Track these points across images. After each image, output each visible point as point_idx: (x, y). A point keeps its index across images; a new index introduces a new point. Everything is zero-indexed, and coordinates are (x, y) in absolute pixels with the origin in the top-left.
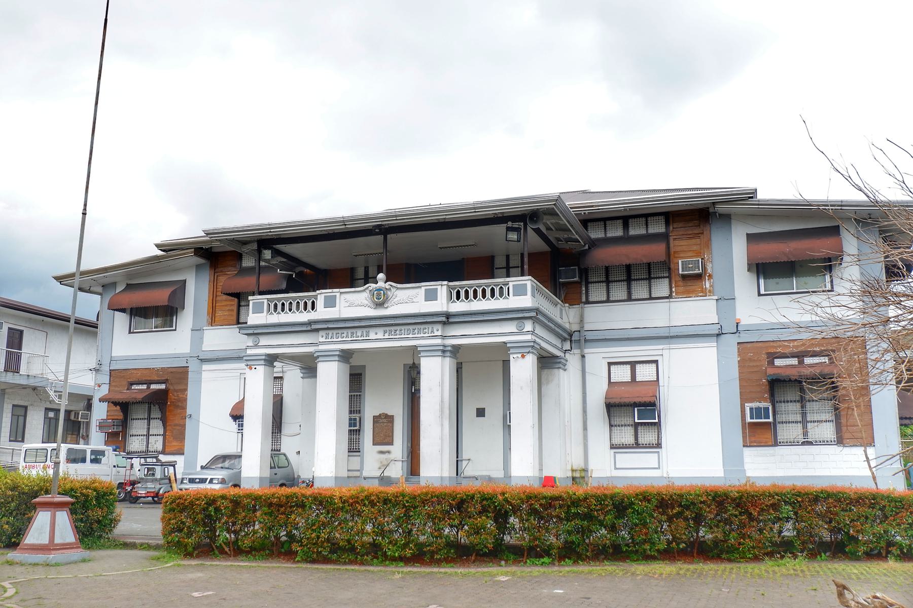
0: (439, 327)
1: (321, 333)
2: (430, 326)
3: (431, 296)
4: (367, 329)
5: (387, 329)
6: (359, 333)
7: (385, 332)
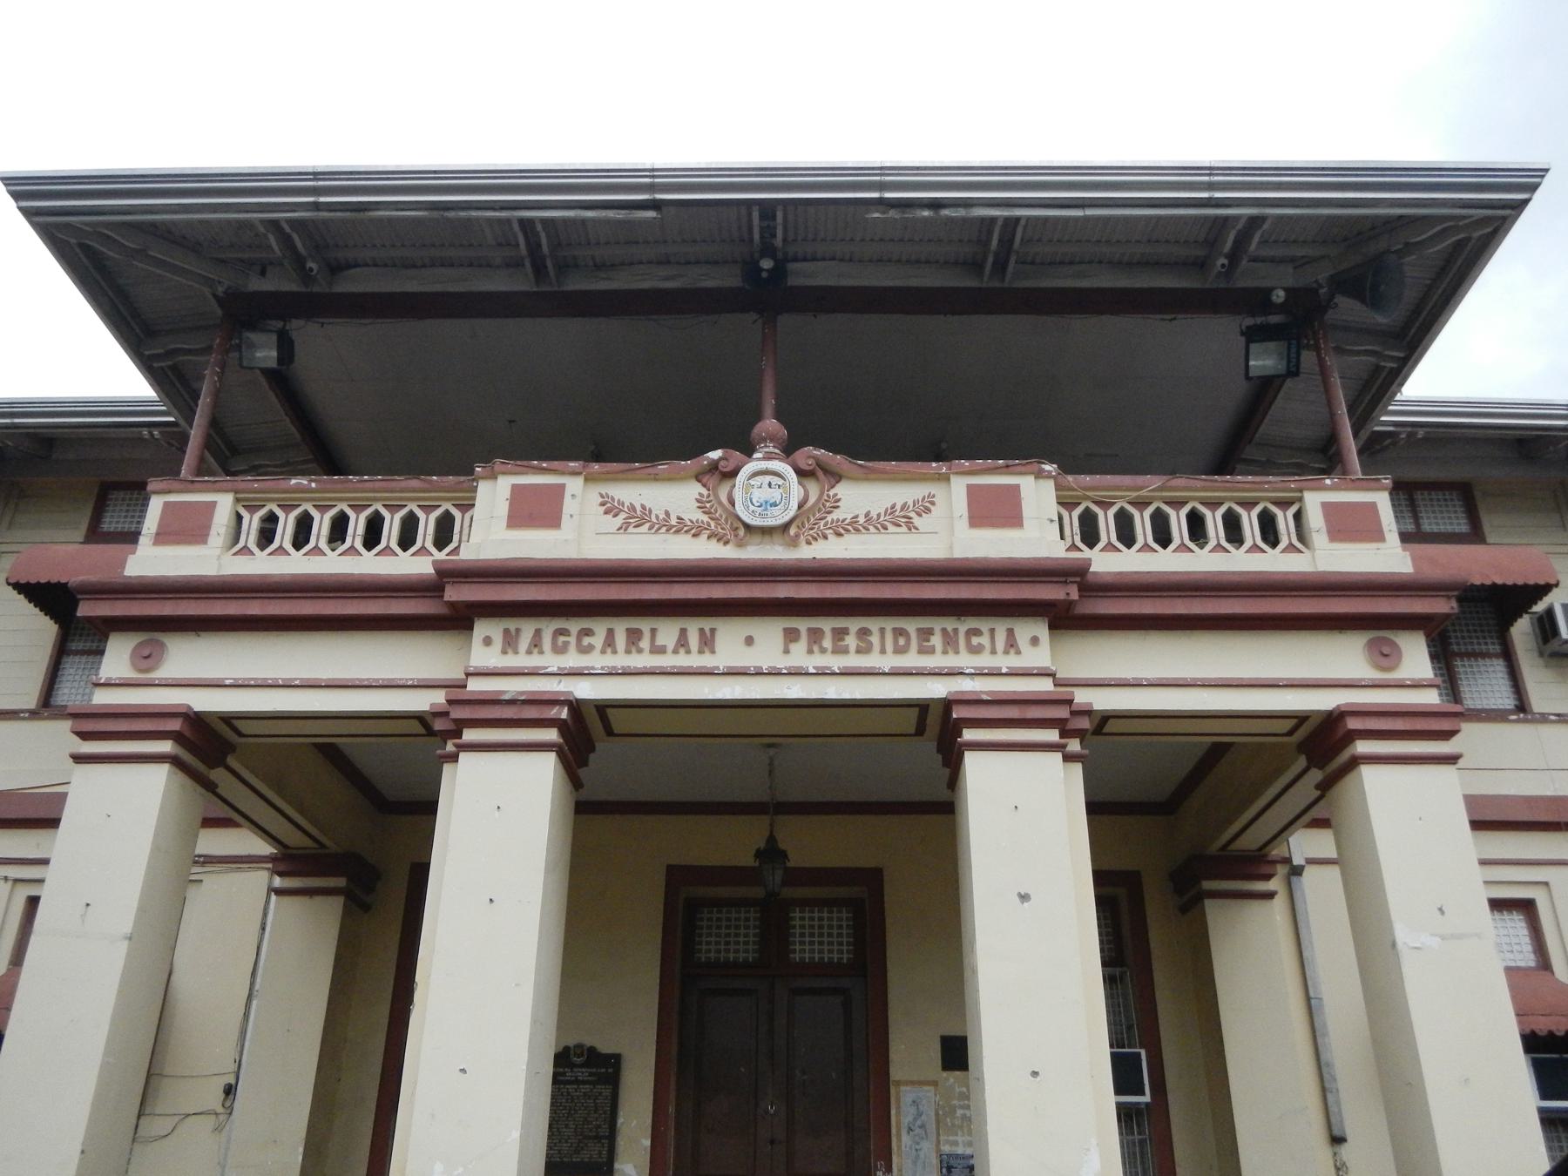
0: (1041, 629)
1: (482, 628)
2: (1001, 627)
3: (996, 510)
4: (707, 623)
5: (803, 624)
6: (668, 631)
7: (791, 636)
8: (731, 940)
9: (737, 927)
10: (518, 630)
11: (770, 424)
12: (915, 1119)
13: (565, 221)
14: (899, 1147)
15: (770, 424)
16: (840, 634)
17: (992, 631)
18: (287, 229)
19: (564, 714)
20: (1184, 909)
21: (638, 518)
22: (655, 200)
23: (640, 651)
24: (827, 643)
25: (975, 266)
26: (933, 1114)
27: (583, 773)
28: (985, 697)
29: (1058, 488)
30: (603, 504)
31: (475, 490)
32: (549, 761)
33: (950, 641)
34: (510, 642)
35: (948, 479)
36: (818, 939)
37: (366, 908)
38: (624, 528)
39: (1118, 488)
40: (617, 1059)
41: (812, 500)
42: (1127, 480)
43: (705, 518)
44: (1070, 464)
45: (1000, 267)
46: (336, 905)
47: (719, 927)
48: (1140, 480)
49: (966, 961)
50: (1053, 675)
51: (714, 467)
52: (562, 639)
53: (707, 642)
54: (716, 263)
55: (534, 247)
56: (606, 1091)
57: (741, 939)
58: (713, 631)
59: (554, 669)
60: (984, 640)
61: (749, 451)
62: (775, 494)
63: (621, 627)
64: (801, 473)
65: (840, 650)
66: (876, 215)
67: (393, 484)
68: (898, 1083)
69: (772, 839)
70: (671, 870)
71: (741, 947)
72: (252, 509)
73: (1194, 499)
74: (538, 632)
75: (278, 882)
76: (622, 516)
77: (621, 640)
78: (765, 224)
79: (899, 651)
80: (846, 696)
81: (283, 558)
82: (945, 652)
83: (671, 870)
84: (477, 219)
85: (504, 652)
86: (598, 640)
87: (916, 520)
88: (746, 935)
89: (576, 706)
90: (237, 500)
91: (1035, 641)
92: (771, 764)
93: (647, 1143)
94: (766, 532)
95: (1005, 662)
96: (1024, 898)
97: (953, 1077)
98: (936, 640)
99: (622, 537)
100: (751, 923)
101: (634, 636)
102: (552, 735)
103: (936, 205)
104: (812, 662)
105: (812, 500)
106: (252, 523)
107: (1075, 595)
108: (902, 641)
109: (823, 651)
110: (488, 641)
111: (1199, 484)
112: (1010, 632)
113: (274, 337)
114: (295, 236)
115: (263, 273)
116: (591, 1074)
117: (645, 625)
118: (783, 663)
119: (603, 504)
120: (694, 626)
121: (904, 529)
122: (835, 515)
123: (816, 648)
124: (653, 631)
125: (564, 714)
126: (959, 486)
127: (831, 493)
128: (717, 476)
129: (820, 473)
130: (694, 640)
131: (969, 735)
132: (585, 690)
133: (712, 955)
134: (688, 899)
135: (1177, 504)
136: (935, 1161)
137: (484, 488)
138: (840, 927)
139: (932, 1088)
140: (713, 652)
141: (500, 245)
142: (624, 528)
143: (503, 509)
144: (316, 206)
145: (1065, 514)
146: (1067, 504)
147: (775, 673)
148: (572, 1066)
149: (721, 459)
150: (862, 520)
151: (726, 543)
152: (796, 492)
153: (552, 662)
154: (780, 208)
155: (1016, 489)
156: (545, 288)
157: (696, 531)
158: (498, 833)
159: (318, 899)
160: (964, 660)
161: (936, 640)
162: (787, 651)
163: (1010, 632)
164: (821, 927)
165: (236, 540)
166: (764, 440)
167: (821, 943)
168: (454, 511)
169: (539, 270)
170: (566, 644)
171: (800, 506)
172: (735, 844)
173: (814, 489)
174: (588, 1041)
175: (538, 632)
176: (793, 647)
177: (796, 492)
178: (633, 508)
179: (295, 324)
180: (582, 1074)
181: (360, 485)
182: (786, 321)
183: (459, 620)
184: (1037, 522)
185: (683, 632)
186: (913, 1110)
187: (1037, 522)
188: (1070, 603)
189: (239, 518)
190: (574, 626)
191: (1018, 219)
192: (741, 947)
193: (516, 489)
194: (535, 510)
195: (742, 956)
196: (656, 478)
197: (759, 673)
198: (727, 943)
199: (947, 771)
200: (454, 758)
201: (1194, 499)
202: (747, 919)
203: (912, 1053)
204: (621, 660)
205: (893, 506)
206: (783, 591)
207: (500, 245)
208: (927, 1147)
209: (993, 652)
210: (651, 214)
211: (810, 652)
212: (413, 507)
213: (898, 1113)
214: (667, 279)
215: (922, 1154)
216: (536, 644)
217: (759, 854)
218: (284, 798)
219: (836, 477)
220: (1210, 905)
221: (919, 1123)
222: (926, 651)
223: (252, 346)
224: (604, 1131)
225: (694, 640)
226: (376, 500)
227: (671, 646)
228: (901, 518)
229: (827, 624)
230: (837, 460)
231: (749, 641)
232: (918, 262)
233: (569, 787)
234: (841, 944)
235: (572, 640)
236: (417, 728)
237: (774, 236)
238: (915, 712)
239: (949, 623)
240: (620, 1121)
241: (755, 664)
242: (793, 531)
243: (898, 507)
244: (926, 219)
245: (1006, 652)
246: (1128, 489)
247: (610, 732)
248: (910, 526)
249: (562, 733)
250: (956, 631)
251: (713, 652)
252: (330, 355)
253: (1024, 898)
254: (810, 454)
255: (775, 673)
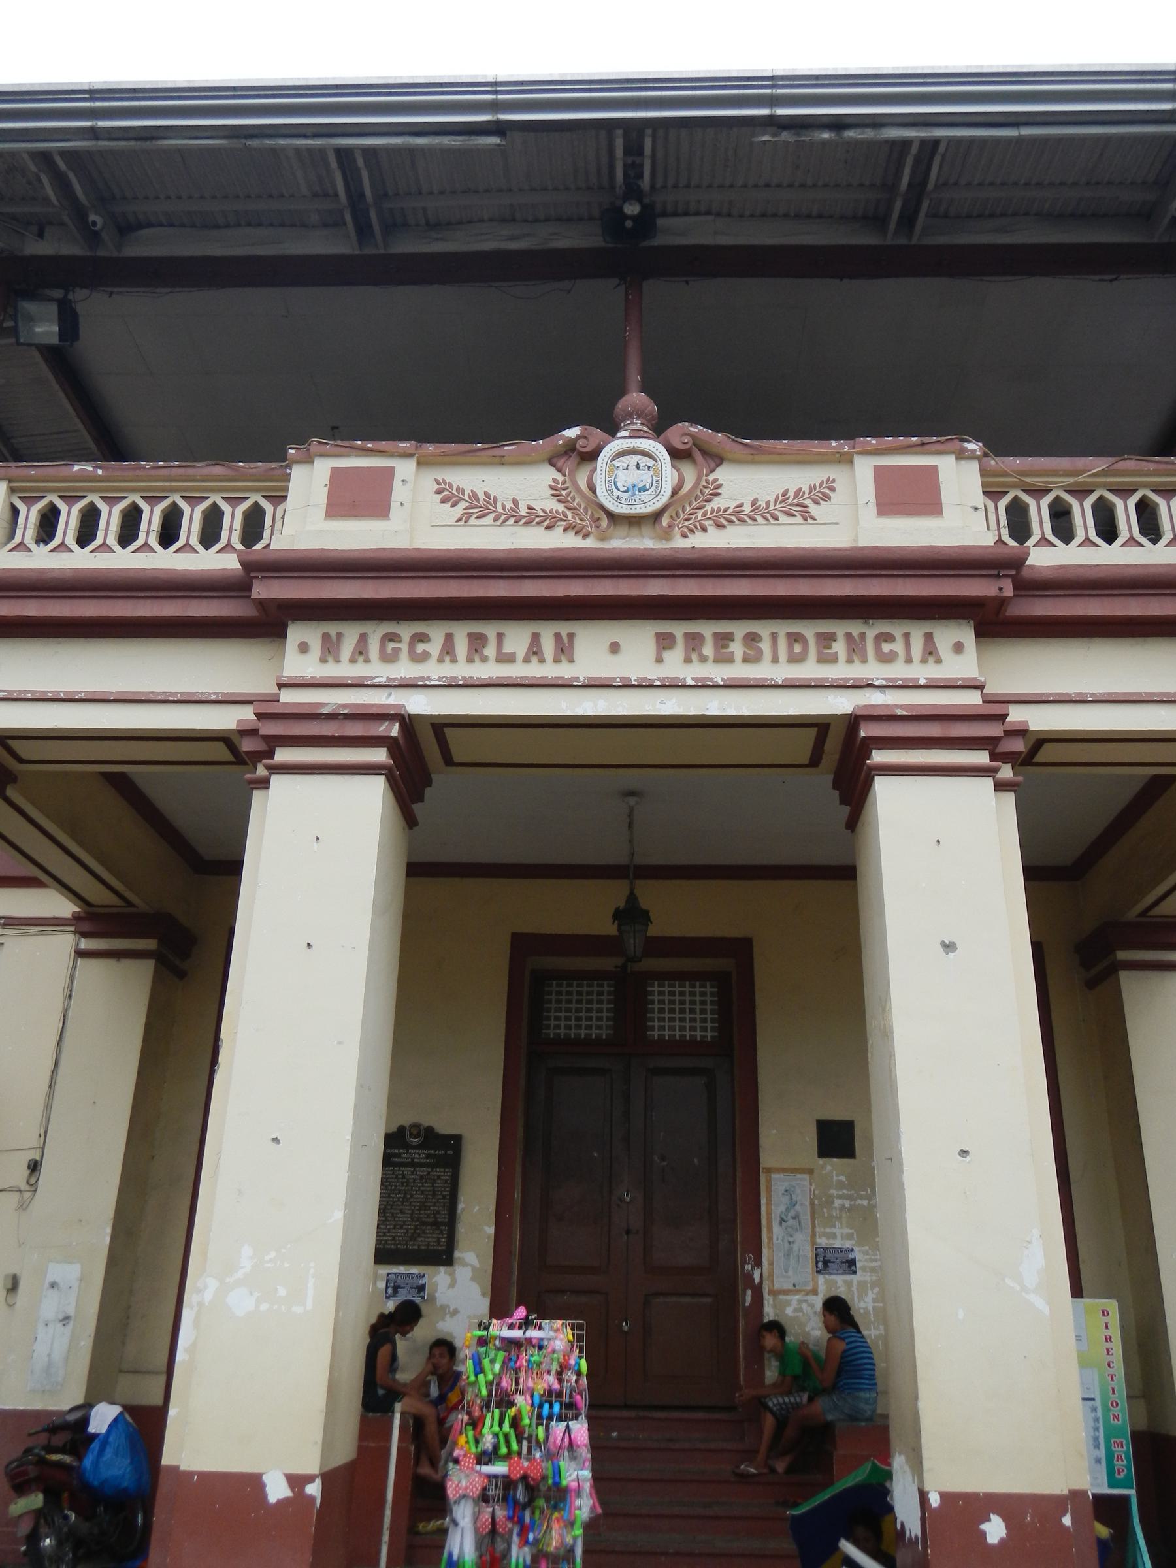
0: (965, 634)
1: (296, 633)
2: (917, 631)
3: (910, 495)
4: (564, 628)
5: (679, 629)
6: (517, 636)
7: (665, 642)
8: (583, 1015)
9: (589, 1002)
10: (339, 635)
11: (636, 398)
12: (788, 1210)
13: (388, 150)
14: (770, 1239)
15: (636, 398)
16: (723, 639)
17: (907, 636)
18: (62, 165)
19: (395, 731)
20: (1091, 984)
21: (482, 508)
22: (498, 122)
23: (484, 660)
24: (708, 650)
25: (877, 220)
26: (808, 1203)
27: (417, 808)
28: (899, 712)
29: (984, 473)
30: (439, 492)
31: (287, 478)
32: (377, 786)
33: (856, 649)
34: (330, 649)
35: (851, 462)
36: (680, 1014)
37: (181, 975)
38: (464, 519)
39: (1055, 473)
40: (458, 1139)
41: (688, 486)
42: (1064, 463)
43: (561, 508)
44: (1000, 443)
45: (908, 220)
46: (146, 968)
47: (569, 1002)
48: (1080, 462)
49: (872, 1025)
50: (980, 687)
51: (570, 448)
52: (391, 645)
53: (564, 650)
54: (569, 220)
55: (356, 198)
56: (445, 1174)
57: (594, 1015)
58: (571, 636)
59: (382, 680)
60: (898, 647)
61: (612, 430)
62: (645, 478)
63: (461, 631)
64: (677, 455)
65: (725, 659)
66: (765, 138)
67: (190, 471)
68: (769, 1171)
69: (632, 898)
70: (517, 938)
71: (594, 1023)
72: (29, 500)
73: (1145, 485)
74: (363, 638)
75: (84, 944)
76: (462, 505)
77: (461, 647)
78: (629, 160)
79: (794, 659)
80: (732, 711)
81: (65, 555)
82: (850, 661)
83: (517, 938)
84: (283, 149)
85: (323, 660)
86: (434, 647)
87: (813, 509)
88: (599, 1011)
89: (408, 722)
90: (12, 490)
91: (958, 648)
92: (630, 815)
93: (491, 1230)
94: (634, 521)
95: (923, 672)
96: (949, 947)
97: (833, 1167)
98: (839, 647)
99: (462, 530)
100: (605, 997)
101: (477, 643)
102: (380, 756)
103: (838, 124)
104: (691, 673)
105: (688, 486)
106: (30, 516)
107: (1009, 592)
108: (797, 648)
109: (703, 659)
110: (304, 648)
111: (1152, 467)
112: (929, 637)
113: (54, 308)
114: (71, 175)
115: (41, 235)
116: (428, 1156)
117: (489, 629)
118: (655, 673)
119: (439, 492)
120: (548, 632)
121: (799, 519)
122: (717, 503)
123: (694, 657)
124: (500, 637)
125: (395, 731)
126: (864, 469)
127: (711, 478)
128: (574, 459)
129: (697, 455)
130: (548, 646)
131: (879, 757)
132: (418, 704)
133: (562, 1031)
134: (536, 971)
135: (1124, 492)
136: (810, 1254)
137: (298, 474)
138: (703, 1003)
139: (807, 1176)
140: (572, 661)
141: (315, 195)
142: (464, 519)
143: (321, 495)
144: (94, 133)
145: (990, 505)
146: (992, 494)
147: (645, 685)
148: (408, 1147)
149: (578, 437)
150: (747, 509)
151: (586, 536)
152: (669, 476)
153: (380, 671)
154: (649, 131)
155: (935, 469)
156: (368, 251)
157: (550, 522)
158: (317, 874)
159: (127, 963)
160: (873, 670)
161: (839, 647)
162: (659, 660)
163: (929, 637)
164: (682, 1002)
165: (12, 536)
166: (630, 415)
167: (682, 1020)
168: (265, 504)
169: (363, 231)
170: (397, 651)
171: (674, 493)
172: (589, 911)
173: (690, 474)
174: (426, 1121)
175: (363, 638)
176: (667, 655)
177: (669, 476)
178: (474, 495)
179: (79, 294)
180: (419, 1155)
181: (153, 472)
182: (653, 288)
183: (269, 626)
184: (961, 508)
185: (536, 637)
186: (785, 1200)
187: (961, 508)
188: (1000, 604)
189: (15, 511)
190: (406, 630)
191: (936, 142)
192: (594, 1023)
193: (334, 471)
194: (359, 498)
195: (594, 1033)
196: (502, 462)
197: (627, 686)
198: (578, 1019)
199: (846, 810)
200: (264, 784)
201: (1145, 485)
202: (600, 994)
203: (784, 1138)
204: (462, 670)
205: (785, 493)
206: (655, 588)
207: (315, 195)
208: (802, 1244)
209: (909, 660)
210: (494, 140)
211: (688, 660)
212: (216, 498)
213: (769, 1203)
214: (512, 238)
215: (795, 1247)
216: (361, 651)
217: (618, 915)
218: (81, 844)
219: (718, 460)
220: (1124, 976)
221: (792, 1213)
222: (827, 659)
223: (30, 319)
224: (443, 1217)
225: (548, 646)
226: (173, 490)
227: (521, 655)
228: (796, 507)
229: (708, 629)
230: (719, 439)
231: (615, 648)
232: (809, 216)
233: (401, 822)
234: (704, 1020)
235: (404, 647)
236: (221, 752)
237: (640, 176)
238: (813, 731)
239: (855, 628)
240: (461, 1206)
241: (620, 675)
242: (665, 521)
243: (791, 494)
244: (824, 143)
245: (924, 661)
246: (1067, 474)
247: (449, 761)
248: (806, 516)
249: (392, 754)
250: (863, 636)
251: (572, 661)
252: (123, 333)
253: (949, 947)
254: (684, 432)
255: (645, 685)
